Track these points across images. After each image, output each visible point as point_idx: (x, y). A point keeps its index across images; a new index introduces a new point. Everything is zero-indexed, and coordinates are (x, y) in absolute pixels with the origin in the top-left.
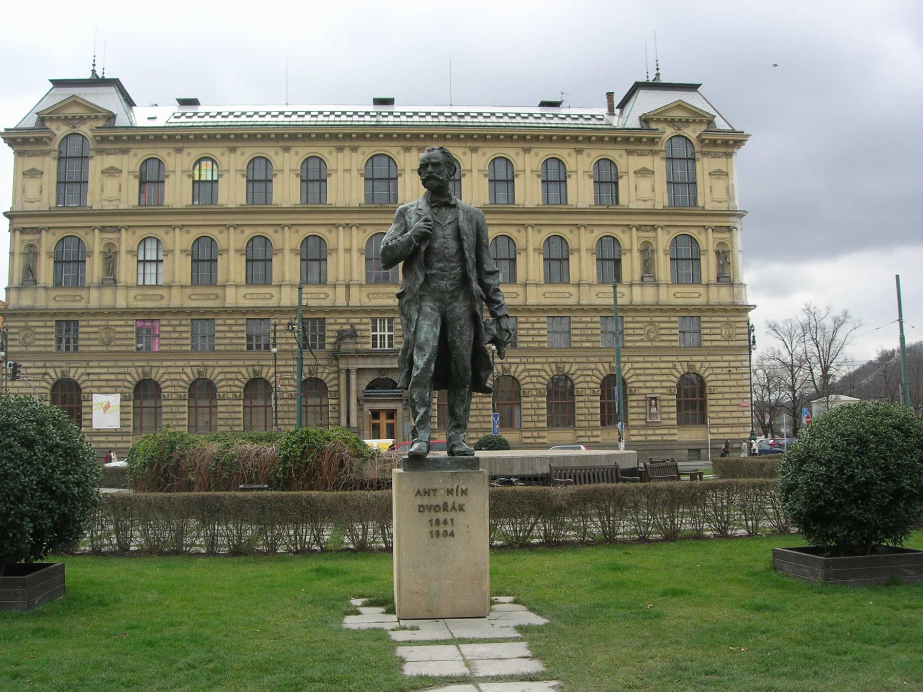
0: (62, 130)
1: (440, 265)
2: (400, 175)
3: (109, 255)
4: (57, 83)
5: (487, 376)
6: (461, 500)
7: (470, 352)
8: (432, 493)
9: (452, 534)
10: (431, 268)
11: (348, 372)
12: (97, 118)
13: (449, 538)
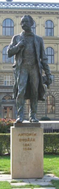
1: (28, 56)
2: (15, 26)
5: (43, 95)
6: (35, 137)
8: (24, 135)
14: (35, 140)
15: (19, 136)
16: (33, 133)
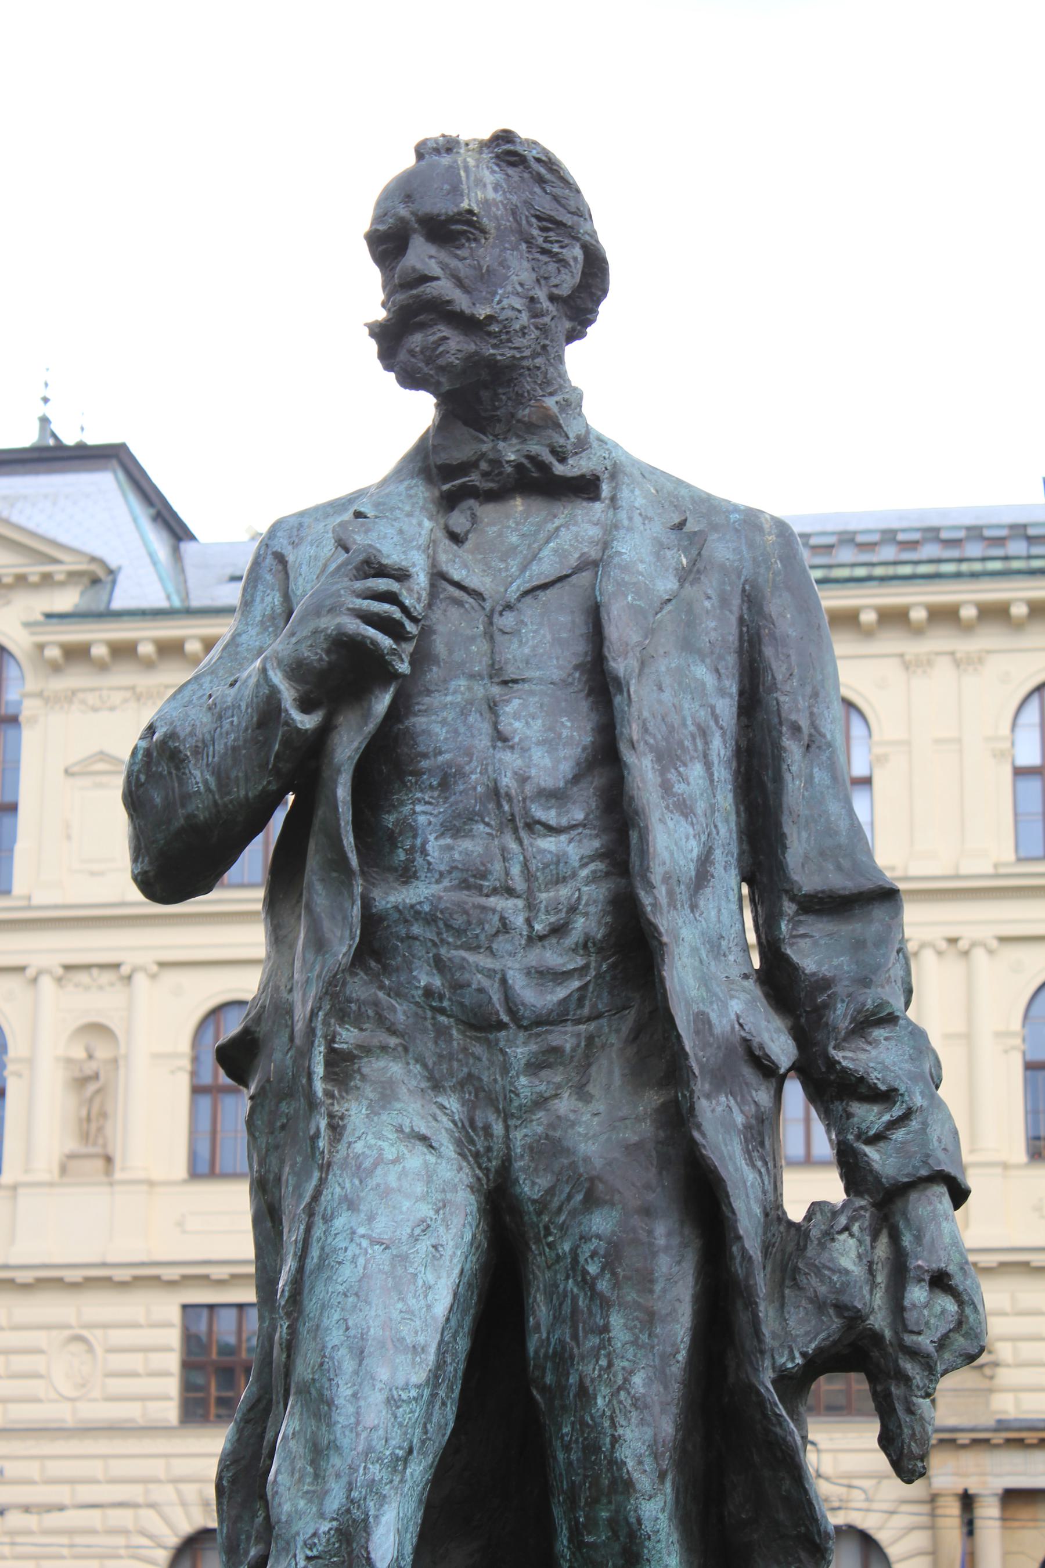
3: (90, 1068)
7: (668, 1427)
10: (407, 875)
11: (967, 1500)
12: (47, 580)
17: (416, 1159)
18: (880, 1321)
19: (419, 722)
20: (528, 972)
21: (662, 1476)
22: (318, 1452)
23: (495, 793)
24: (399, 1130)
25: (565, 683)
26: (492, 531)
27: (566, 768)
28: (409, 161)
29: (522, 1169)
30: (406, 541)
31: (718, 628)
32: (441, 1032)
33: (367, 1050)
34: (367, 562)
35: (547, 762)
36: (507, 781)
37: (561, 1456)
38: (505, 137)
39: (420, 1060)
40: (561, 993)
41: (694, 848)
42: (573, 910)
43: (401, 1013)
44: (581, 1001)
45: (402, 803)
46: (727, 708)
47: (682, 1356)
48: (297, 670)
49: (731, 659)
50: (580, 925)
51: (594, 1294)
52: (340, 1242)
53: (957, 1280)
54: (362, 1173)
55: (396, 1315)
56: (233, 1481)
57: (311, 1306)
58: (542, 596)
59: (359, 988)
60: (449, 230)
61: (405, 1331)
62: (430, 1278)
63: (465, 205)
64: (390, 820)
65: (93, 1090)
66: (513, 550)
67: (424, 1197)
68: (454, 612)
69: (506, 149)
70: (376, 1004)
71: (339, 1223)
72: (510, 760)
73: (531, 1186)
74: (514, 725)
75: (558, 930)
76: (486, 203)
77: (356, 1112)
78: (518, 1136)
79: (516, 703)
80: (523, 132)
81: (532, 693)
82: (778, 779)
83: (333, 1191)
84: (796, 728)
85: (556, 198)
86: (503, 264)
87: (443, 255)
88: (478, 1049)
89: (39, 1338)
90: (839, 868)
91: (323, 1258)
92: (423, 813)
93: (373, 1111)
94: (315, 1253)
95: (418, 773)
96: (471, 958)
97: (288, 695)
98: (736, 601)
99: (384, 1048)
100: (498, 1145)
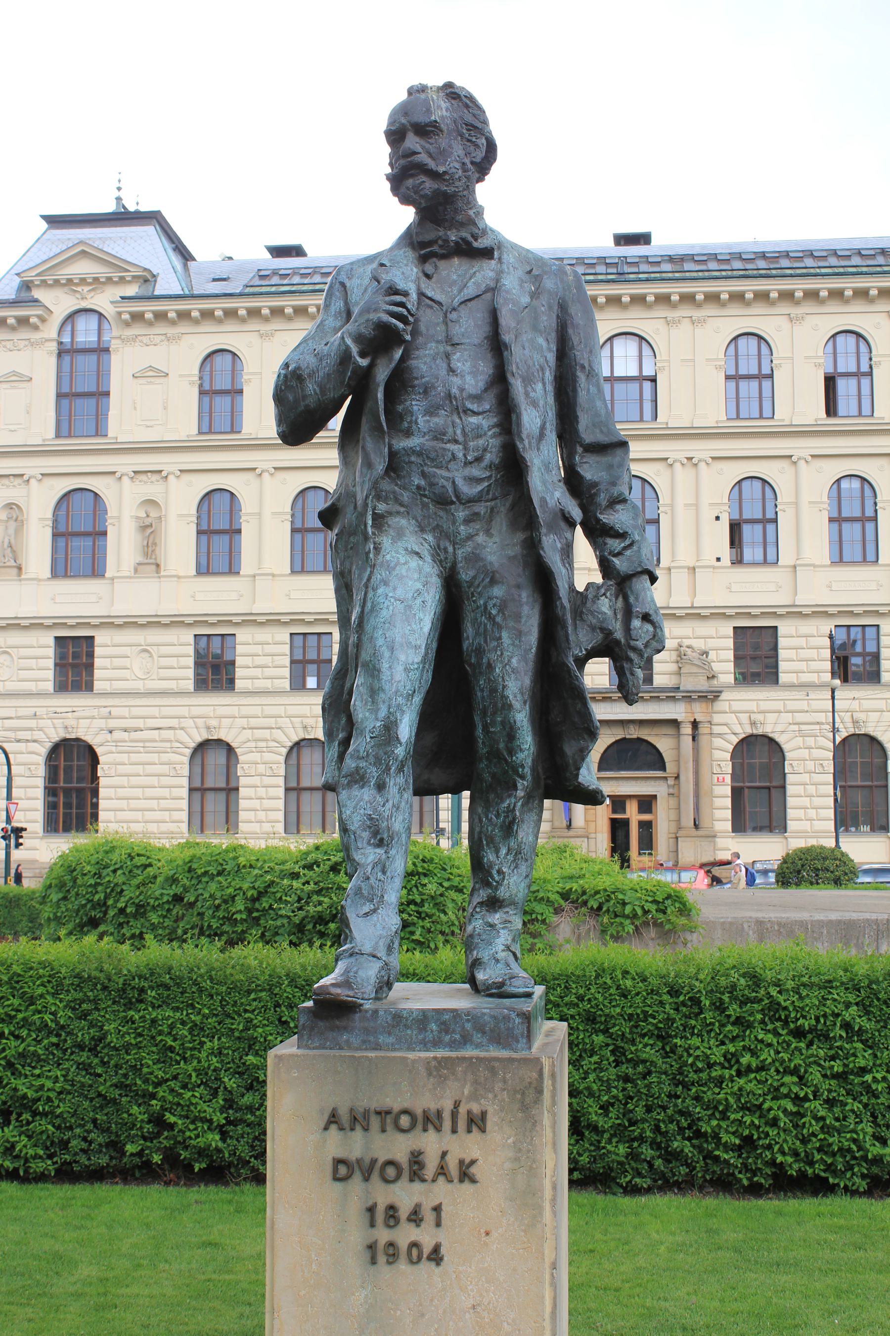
0: (60, 303)
3: (148, 522)
4: (55, 221)
7: (527, 681)
8: (375, 1122)
9: (436, 1256)
10: (408, 433)
13: (426, 1267)
14: (473, 1170)
15: (326, 1128)
16: (457, 1105)
17: (414, 563)
18: (619, 635)
19: (413, 363)
20: (465, 478)
21: (525, 703)
22: (373, 692)
23: (449, 396)
24: (406, 549)
25: (480, 345)
26: (444, 273)
27: (481, 385)
28: (404, 96)
29: (462, 568)
30: (406, 278)
31: (548, 321)
32: (425, 506)
33: (390, 513)
34: (390, 288)
35: (473, 382)
36: (455, 391)
37: (479, 694)
38: (449, 85)
39: (415, 518)
40: (479, 488)
41: (538, 422)
42: (485, 450)
43: (406, 496)
44: (488, 493)
45: (406, 400)
46: (551, 357)
47: (534, 650)
48: (359, 339)
49: (553, 336)
50: (488, 456)
51: (495, 623)
52: (381, 600)
53: (653, 617)
54: (390, 569)
55: (407, 632)
56: (330, 705)
57: (368, 628)
58: (469, 304)
59: (386, 485)
60: (425, 130)
61: (411, 639)
62: (422, 616)
63: (433, 118)
64: (400, 408)
65: (149, 532)
66: (454, 282)
67: (419, 579)
68: (428, 311)
69: (451, 92)
70: (394, 492)
71: (380, 591)
72: (457, 381)
73: (465, 575)
74: (458, 365)
75: (478, 459)
76: (442, 117)
77: (386, 541)
78: (460, 553)
79: (458, 354)
80: (458, 83)
81: (465, 350)
82: (575, 390)
83: (377, 577)
84: (583, 367)
85: (474, 115)
86: (450, 146)
87: (423, 142)
88: (441, 513)
89: (127, 650)
90: (602, 432)
91: (373, 606)
92: (416, 405)
93: (394, 541)
94: (369, 604)
95: (413, 387)
96: (438, 472)
97: (355, 350)
98: (556, 308)
99: (398, 513)
100: (450, 557)
